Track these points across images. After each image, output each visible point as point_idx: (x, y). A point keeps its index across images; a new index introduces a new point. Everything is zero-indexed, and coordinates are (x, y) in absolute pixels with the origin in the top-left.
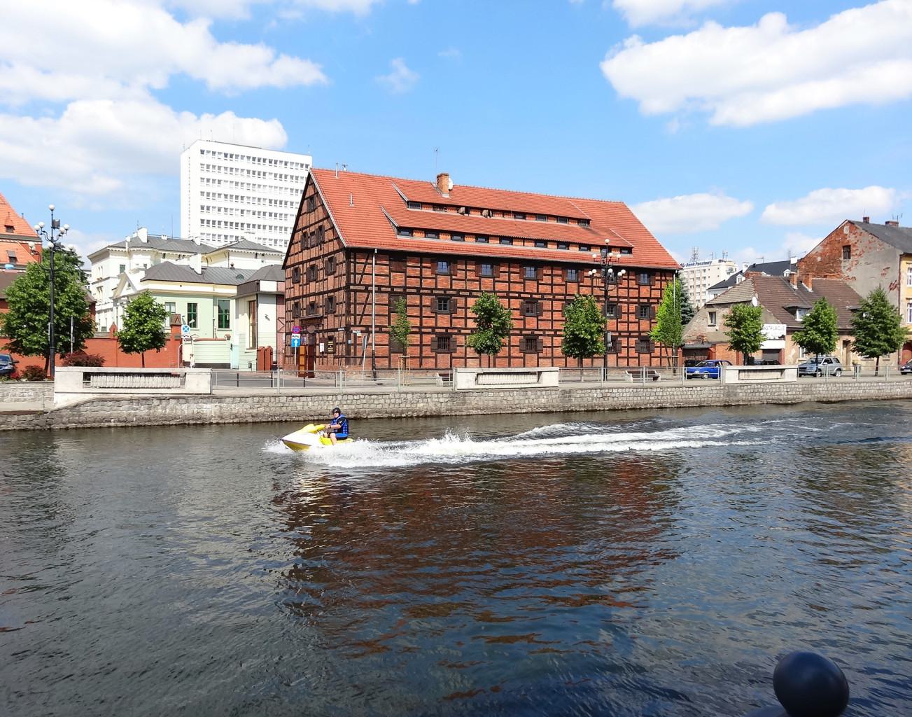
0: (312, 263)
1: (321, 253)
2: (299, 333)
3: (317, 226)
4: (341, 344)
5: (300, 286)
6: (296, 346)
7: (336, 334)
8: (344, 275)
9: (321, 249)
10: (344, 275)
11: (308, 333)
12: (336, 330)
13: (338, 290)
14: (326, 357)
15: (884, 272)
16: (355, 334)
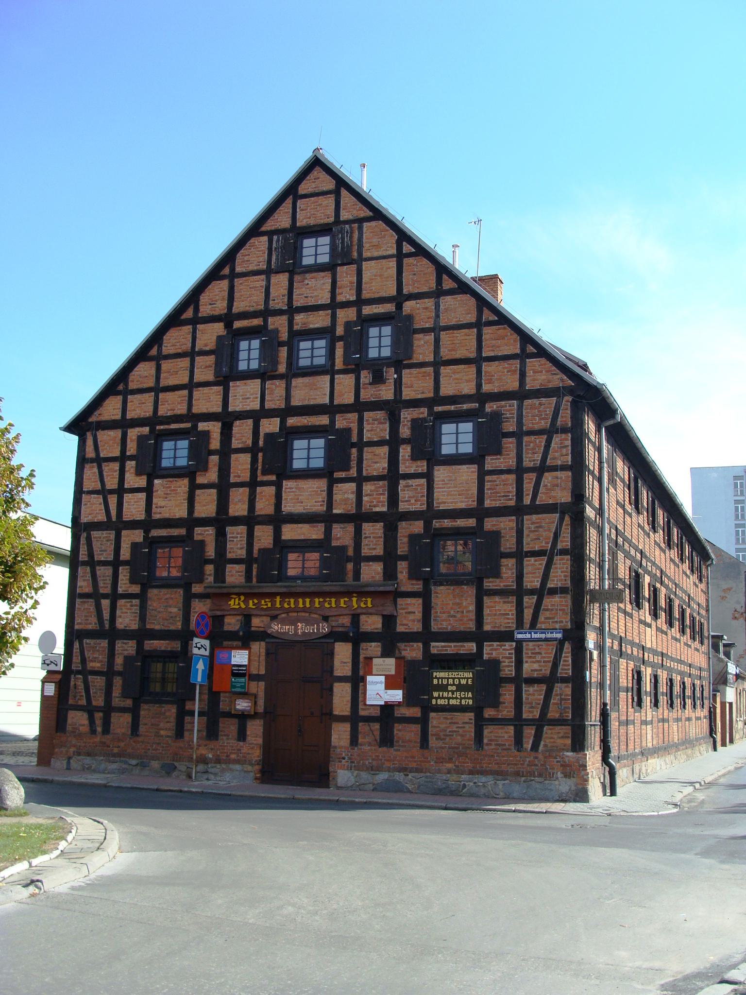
0: (292, 421)
1: (386, 392)
2: (206, 638)
3: (346, 315)
4: (531, 681)
5: (194, 487)
6: (199, 679)
7: (491, 650)
8: (563, 468)
9: (378, 379)
10: (563, 468)
11: (262, 636)
12: (505, 636)
13: (518, 511)
14: (424, 722)
15: (723, 594)
16: (591, 653)
